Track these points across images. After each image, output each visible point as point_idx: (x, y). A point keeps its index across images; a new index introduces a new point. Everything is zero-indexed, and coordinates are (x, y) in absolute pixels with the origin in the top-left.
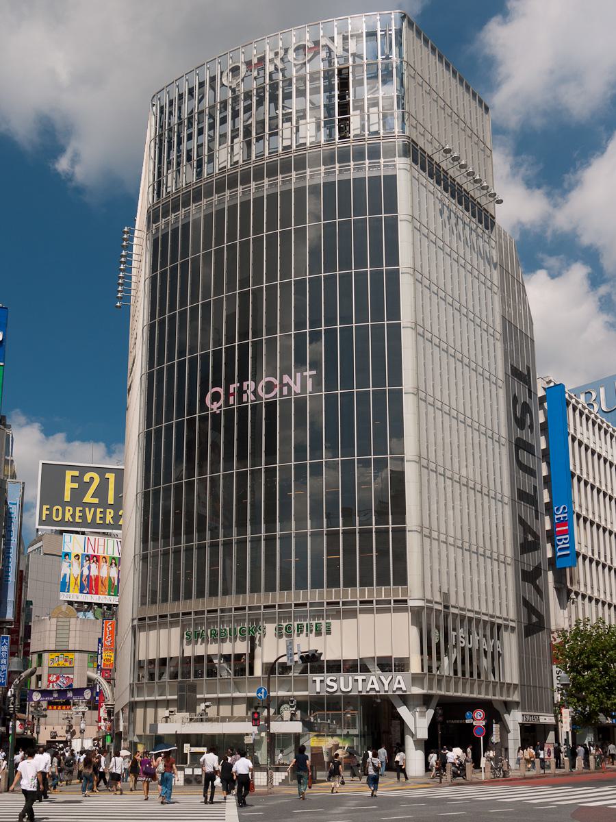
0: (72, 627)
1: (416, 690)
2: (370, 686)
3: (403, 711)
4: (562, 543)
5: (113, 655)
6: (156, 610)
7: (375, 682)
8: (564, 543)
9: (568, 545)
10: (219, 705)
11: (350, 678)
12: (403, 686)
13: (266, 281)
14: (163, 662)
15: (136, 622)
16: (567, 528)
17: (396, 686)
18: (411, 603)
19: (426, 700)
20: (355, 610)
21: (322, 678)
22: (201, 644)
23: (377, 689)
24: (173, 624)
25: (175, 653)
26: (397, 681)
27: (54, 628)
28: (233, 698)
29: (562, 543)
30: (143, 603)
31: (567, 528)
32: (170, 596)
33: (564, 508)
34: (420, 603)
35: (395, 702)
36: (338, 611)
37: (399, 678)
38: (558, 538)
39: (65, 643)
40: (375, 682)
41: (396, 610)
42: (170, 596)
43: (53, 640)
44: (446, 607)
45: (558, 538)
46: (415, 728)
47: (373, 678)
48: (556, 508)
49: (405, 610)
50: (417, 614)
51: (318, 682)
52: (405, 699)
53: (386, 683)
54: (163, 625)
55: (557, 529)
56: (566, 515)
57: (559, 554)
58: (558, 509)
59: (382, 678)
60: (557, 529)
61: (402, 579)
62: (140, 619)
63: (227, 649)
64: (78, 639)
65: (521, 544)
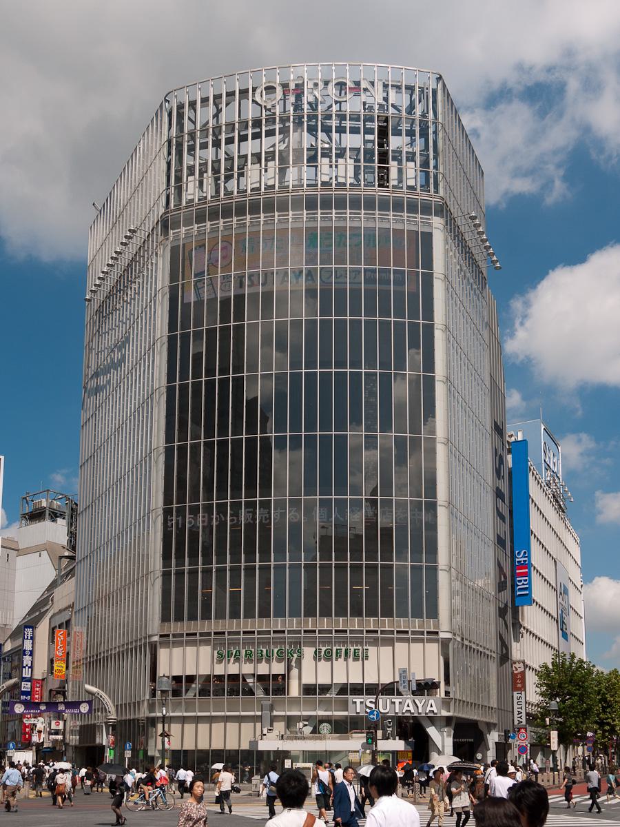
1: (444, 713)
2: (406, 708)
3: (432, 731)
4: (521, 583)
5: (64, 666)
6: (174, 628)
7: (410, 705)
8: (523, 584)
9: (527, 586)
10: (183, 724)
11: (388, 700)
12: (434, 709)
14: (191, 679)
16: (527, 570)
17: (429, 708)
18: (442, 635)
19: (448, 721)
20: (392, 639)
21: (362, 700)
22: (234, 663)
23: (412, 711)
24: (207, 643)
25: (204, 670)
26: (429, 704)
28: (184, 717)
29: (521, 583)
30: (165, 618)
31: (527, 570)
33: (525, 553)
34: (448, 636)
35: (424, 723)
36: (376, 639)
37: (432, 701)
38: (518, 579)
40: (410, 705)
41: (429, 641)
44: (462, 639)
45: (518, 579)
46: (443, 746)
47: (409, 701)
48: (517, 552)
49: (437, 641)
50: (445, 644)
51: (358, 704)
52: (433, 720)
53: (420, 706)
54: (193, 643)
55: (518, 571)
56: (526, 559)
57: (518, 593)
58: (519, 553)
59: (417, 701)
60: (518, 571)
61: (433, 613)
62: (161, 636)
63: (263, 669)
65: (499, 583)
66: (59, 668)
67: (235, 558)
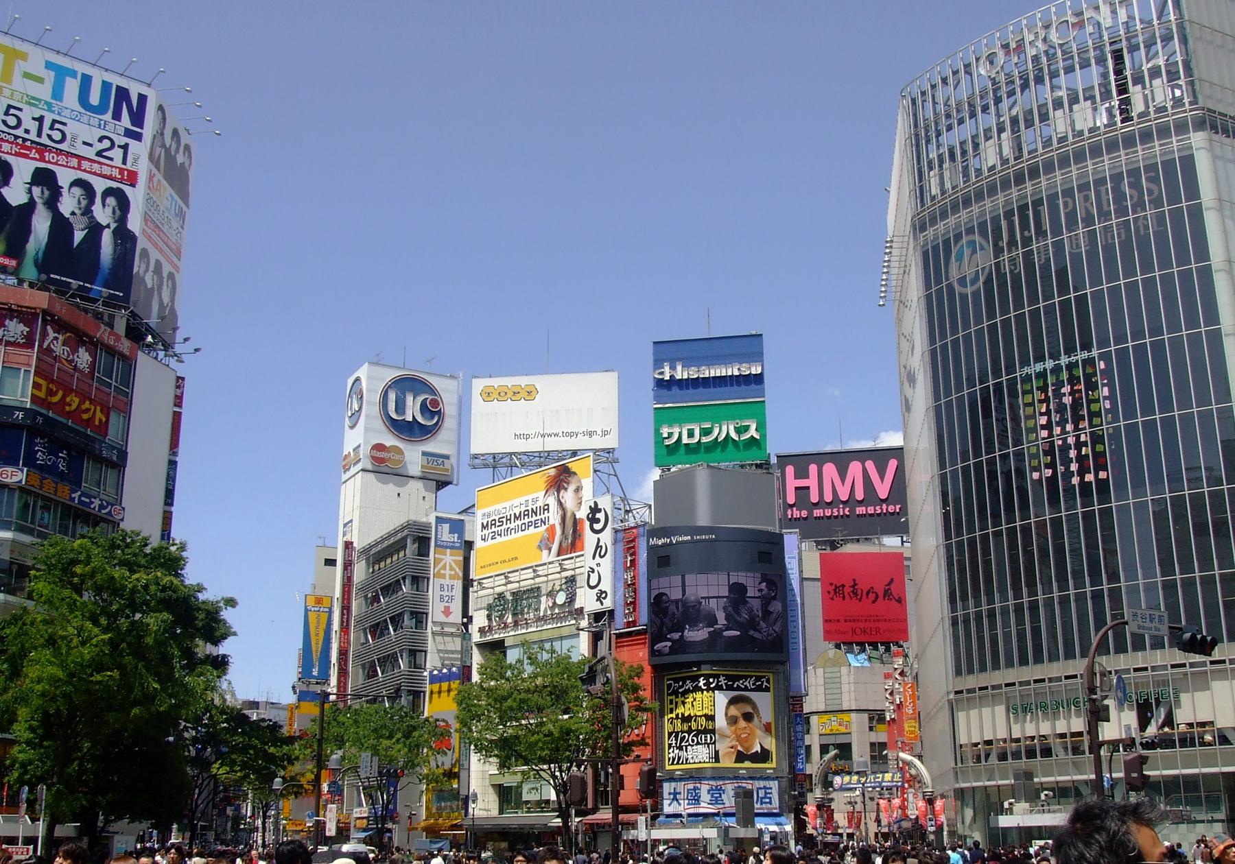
0: (844, 679)
5: (917, 725)
6: (972, 681)
13: (1058, 293)
15: (952, 696)
22: (1031, 722)
24: (994, 700)
27: (821, 681)
30: (958, 672)
32: (989, 664)
39: (836, 701)
42: (989, 664)
43: (821, 698)
54: (982, 702)
62: (957, 693)
64: (853, 694)
66: (911, 729)
67: (1032, 592)
